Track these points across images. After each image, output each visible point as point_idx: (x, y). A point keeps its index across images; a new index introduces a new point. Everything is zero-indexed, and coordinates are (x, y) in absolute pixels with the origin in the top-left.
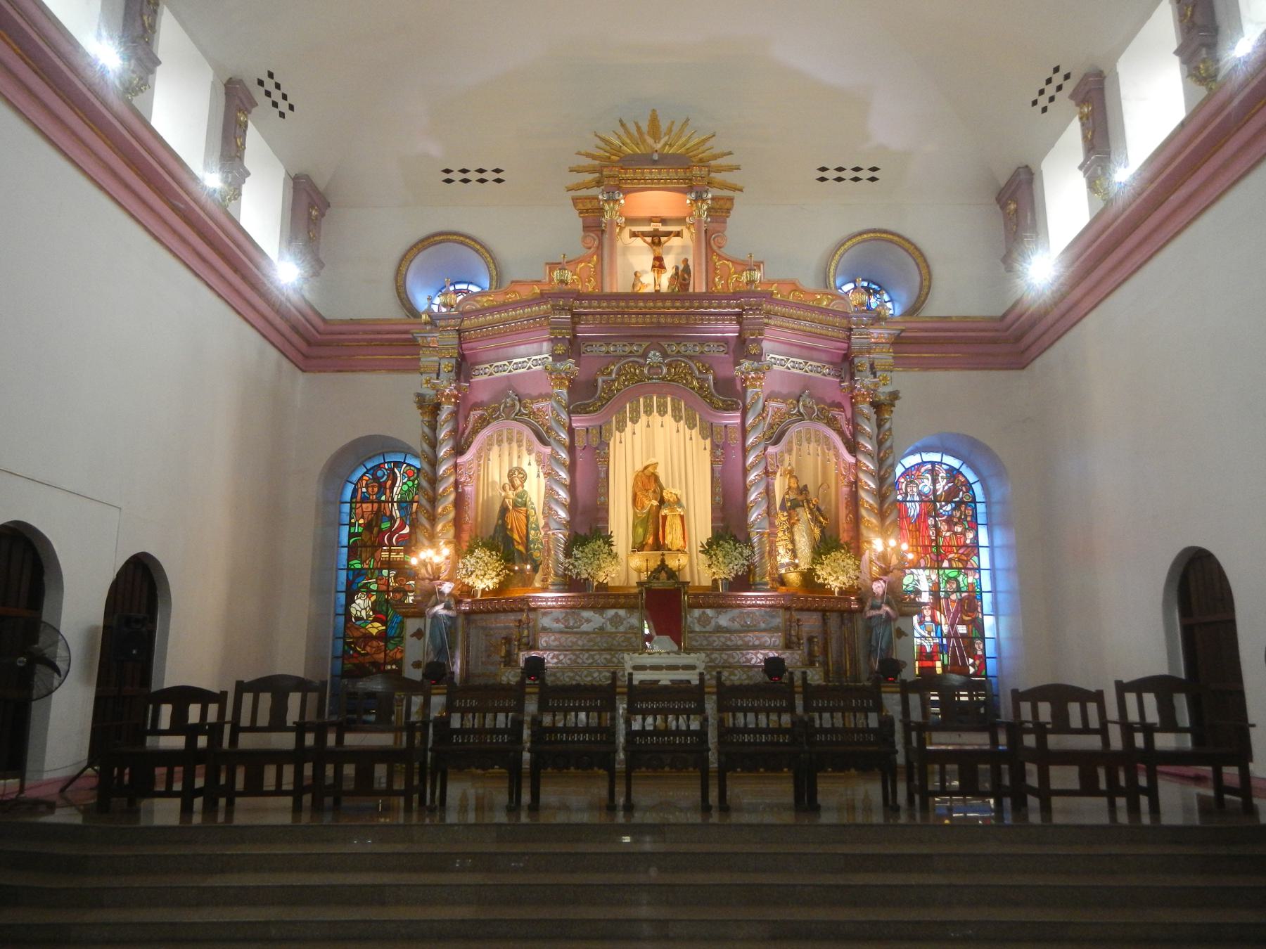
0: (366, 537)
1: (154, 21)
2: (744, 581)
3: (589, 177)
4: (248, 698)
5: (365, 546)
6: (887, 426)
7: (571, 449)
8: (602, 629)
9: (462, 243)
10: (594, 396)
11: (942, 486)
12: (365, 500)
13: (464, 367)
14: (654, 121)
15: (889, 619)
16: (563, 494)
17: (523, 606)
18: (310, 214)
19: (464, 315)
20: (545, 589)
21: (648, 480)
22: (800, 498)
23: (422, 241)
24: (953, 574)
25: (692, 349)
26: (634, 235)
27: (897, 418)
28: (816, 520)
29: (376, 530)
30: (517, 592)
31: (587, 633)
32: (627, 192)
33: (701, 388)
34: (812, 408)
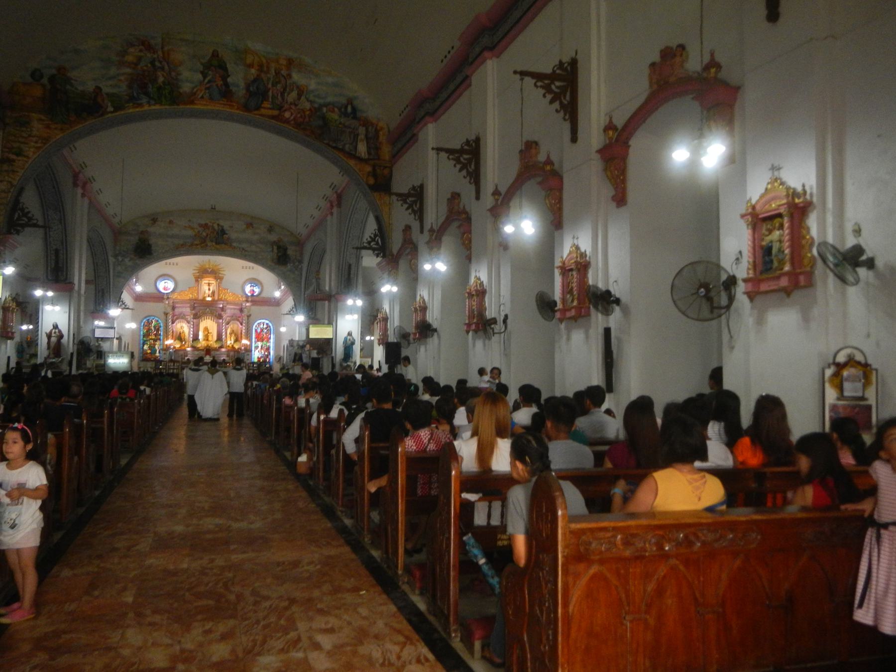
2: (221, 347)
3: (197, 271)
7: (193, 325)
11: (265, 326)
13: (174, 308)
14: (209, 261)
15: (244, 353)
16: (192, 333)
17: (185, 350)
19: (174, 300)
20: (188, 347)
21: (206, 329)
22: (232, 332)
24: (265, 343)
25: (214, 308)
27: (251, 317)
28: (235, 336)
30: (183, 348)
32: (203, 278)
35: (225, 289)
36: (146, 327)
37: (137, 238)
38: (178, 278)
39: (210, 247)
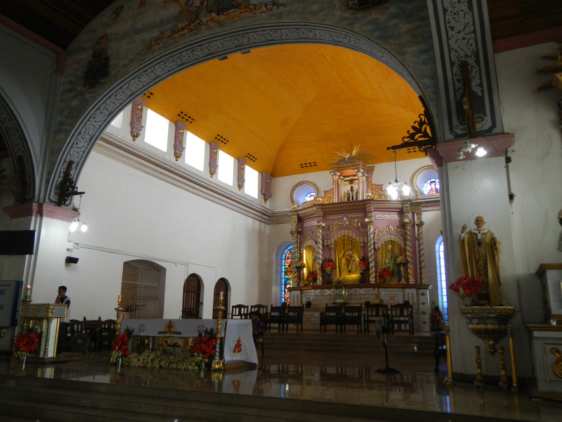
0: (289, 269)
1: (216, 157)
4: (234, 309)
5: (289, 271)
6: (420, 231)
8: (330, 294)
9: (307, 184)
10: (329, 230)
12: (288, 258)
18: (267, 182)
23: (296, 185)
26: (345, 181)
29: (291, 267)
31: (325, 295)
33: (357, 226)
34: (391, 229)
35: (379, 186)
36: (289, 260)
37: (91, 52)
38: (319, 184)
39: (206, 24)
